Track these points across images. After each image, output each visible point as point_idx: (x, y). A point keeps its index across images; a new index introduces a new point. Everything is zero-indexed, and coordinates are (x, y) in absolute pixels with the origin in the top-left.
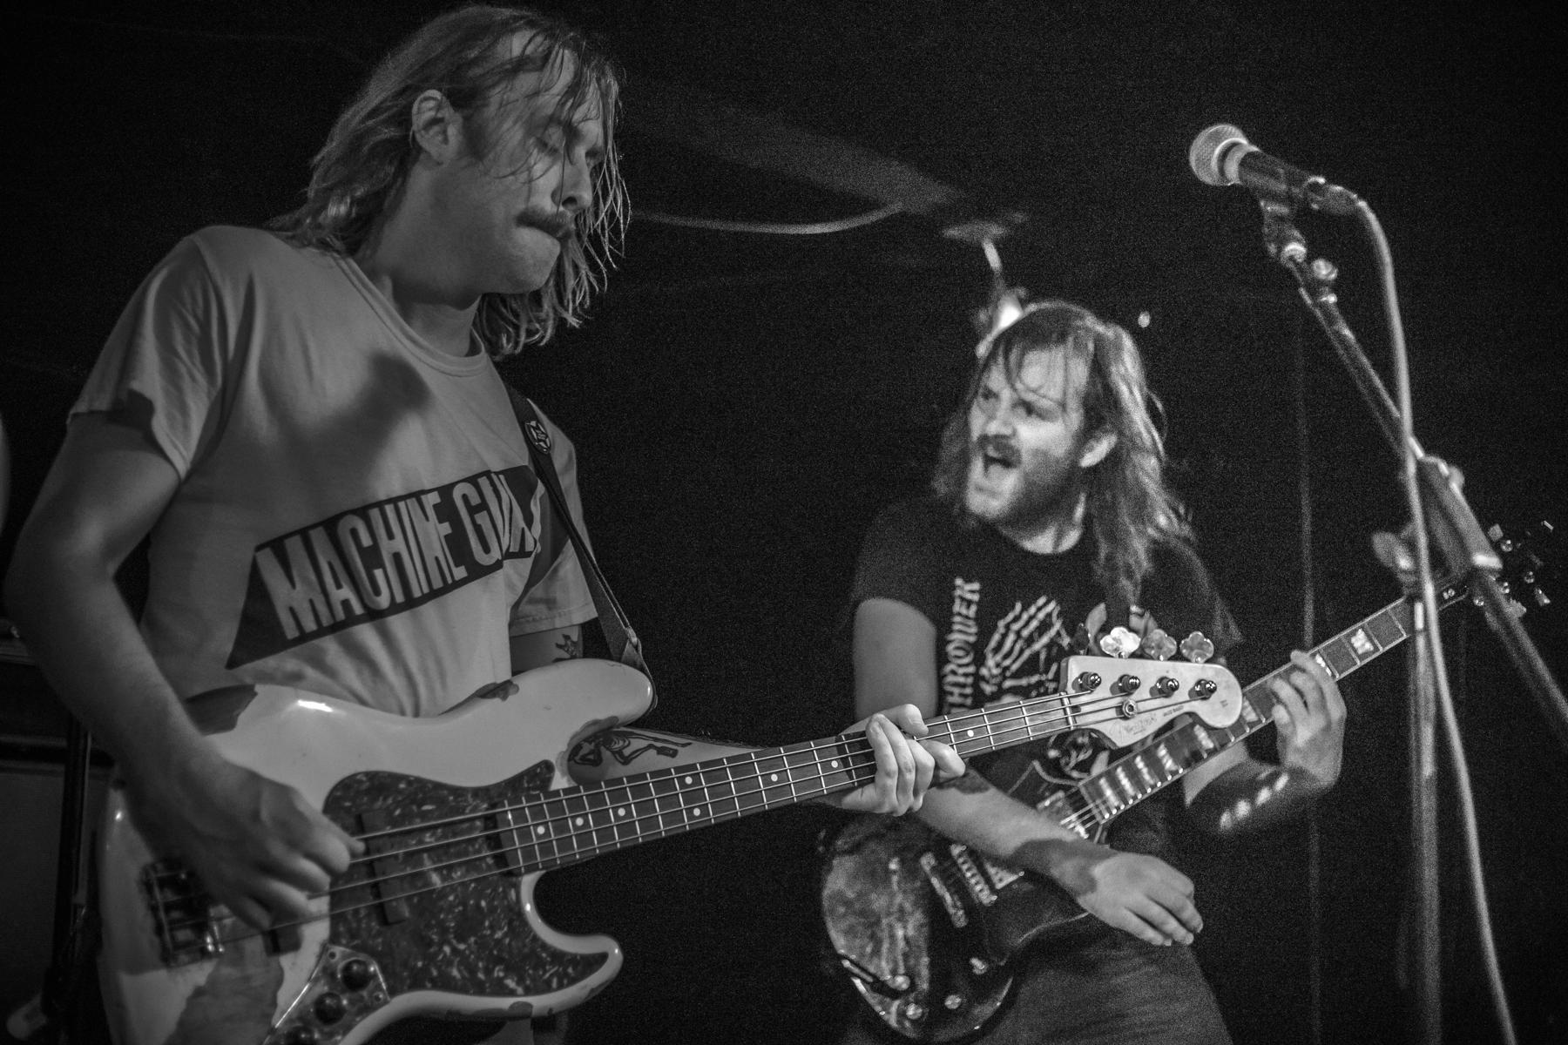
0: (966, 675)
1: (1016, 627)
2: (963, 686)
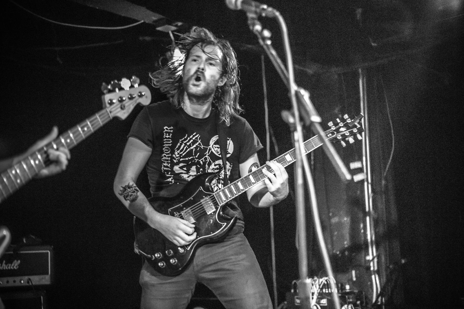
0: (168, 157)
1: (185, 142)
2: (168, 160)
